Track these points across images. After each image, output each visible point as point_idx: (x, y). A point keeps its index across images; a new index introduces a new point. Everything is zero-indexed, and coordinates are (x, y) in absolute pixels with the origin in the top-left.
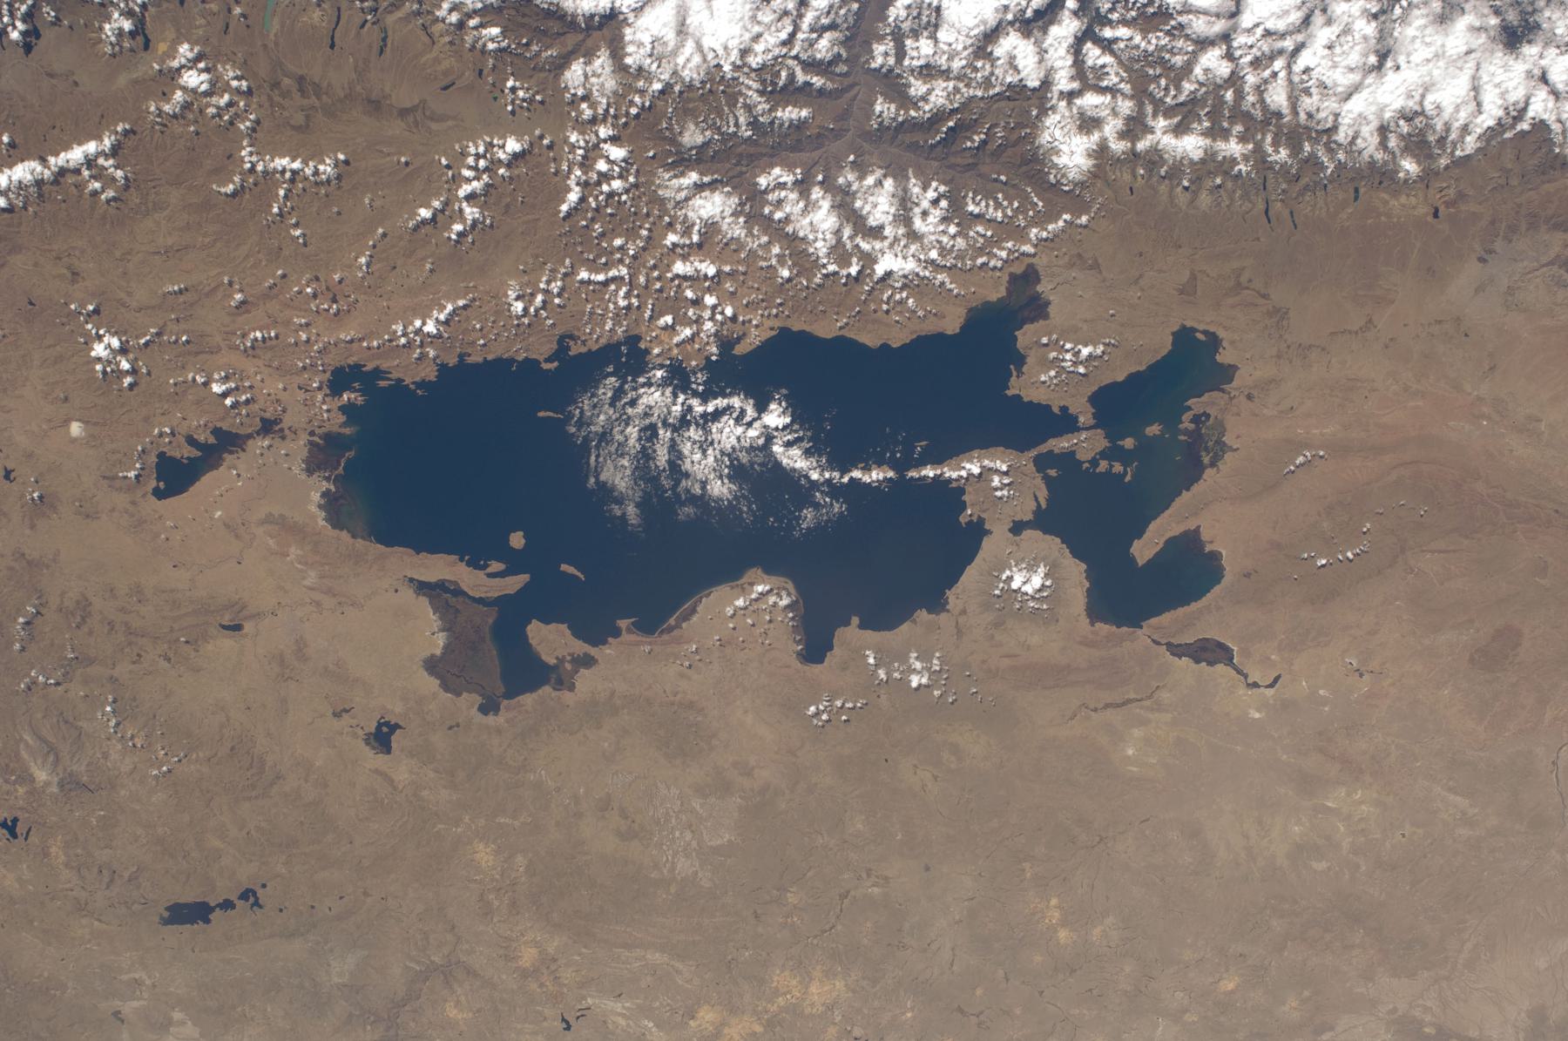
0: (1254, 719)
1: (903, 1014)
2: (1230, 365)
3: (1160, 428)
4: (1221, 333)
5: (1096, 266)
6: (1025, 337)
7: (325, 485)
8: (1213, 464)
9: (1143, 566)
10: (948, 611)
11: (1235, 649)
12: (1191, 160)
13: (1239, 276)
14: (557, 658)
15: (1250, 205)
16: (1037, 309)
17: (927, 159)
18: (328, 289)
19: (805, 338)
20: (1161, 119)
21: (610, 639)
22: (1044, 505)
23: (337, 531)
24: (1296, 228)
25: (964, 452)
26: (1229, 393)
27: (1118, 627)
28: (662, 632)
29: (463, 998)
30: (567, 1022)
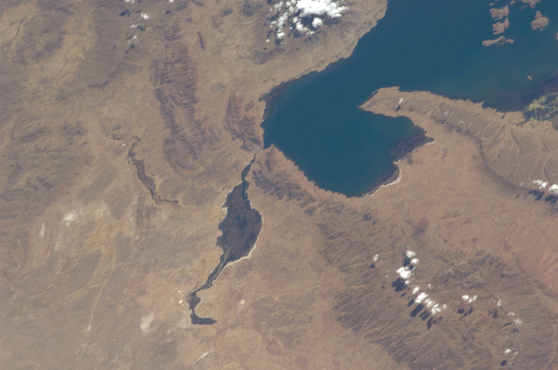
11: (250, 255)
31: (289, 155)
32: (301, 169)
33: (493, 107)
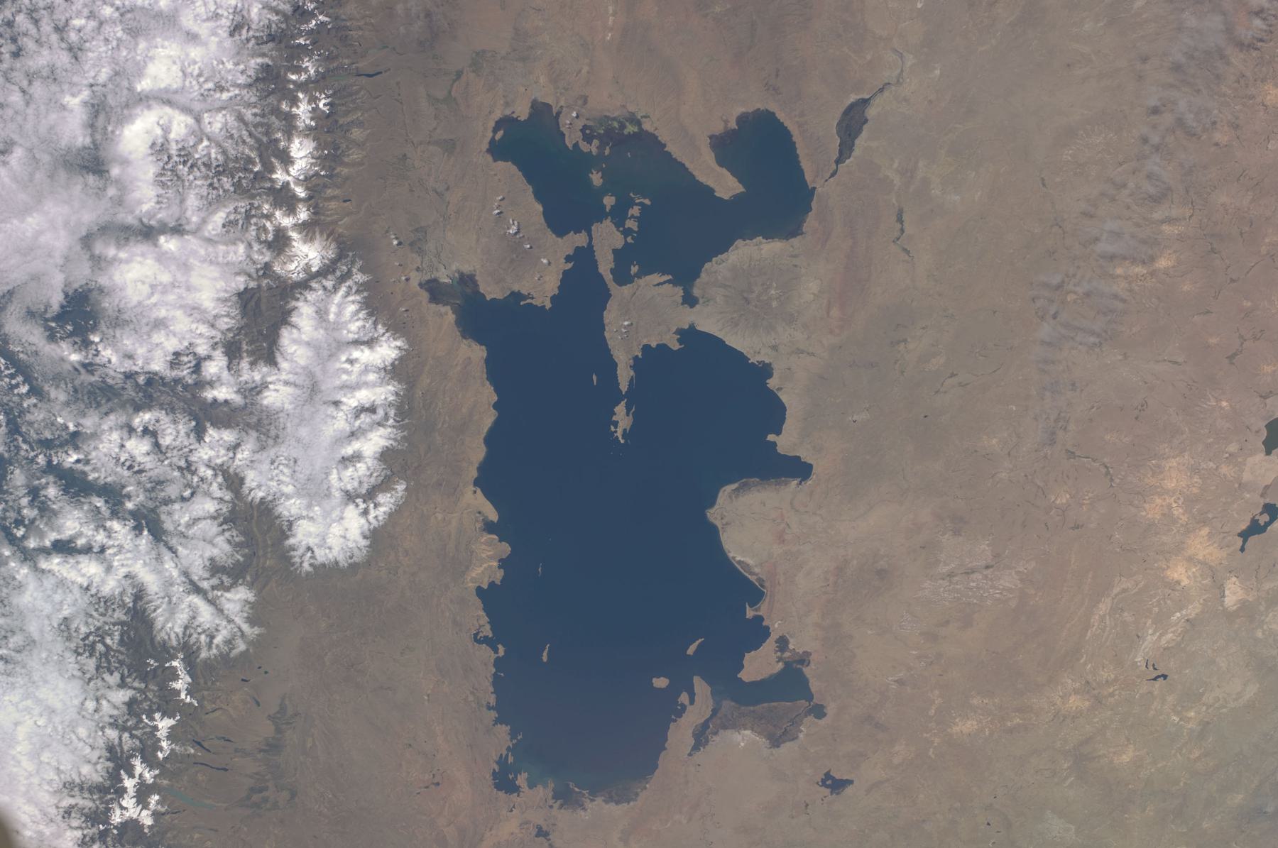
1: (1222, 408)
2: (532, 107)
3: (594, 172)
4: (497, 115)
6: (492, 291)
8: (639, 123)
9: (744, 186)
12: (316, 149)
14: (778, 662)
15: (362, 93)
16: (466, 280)
18: (427, 787)
20: (274, 176)
21: (764, 624)
22: (670, 277)
25: (607, 344)
26: (562, 107)
28: (762, 586)
29: (1112, 750)
30: (1159, 677)
33: (660, 142)
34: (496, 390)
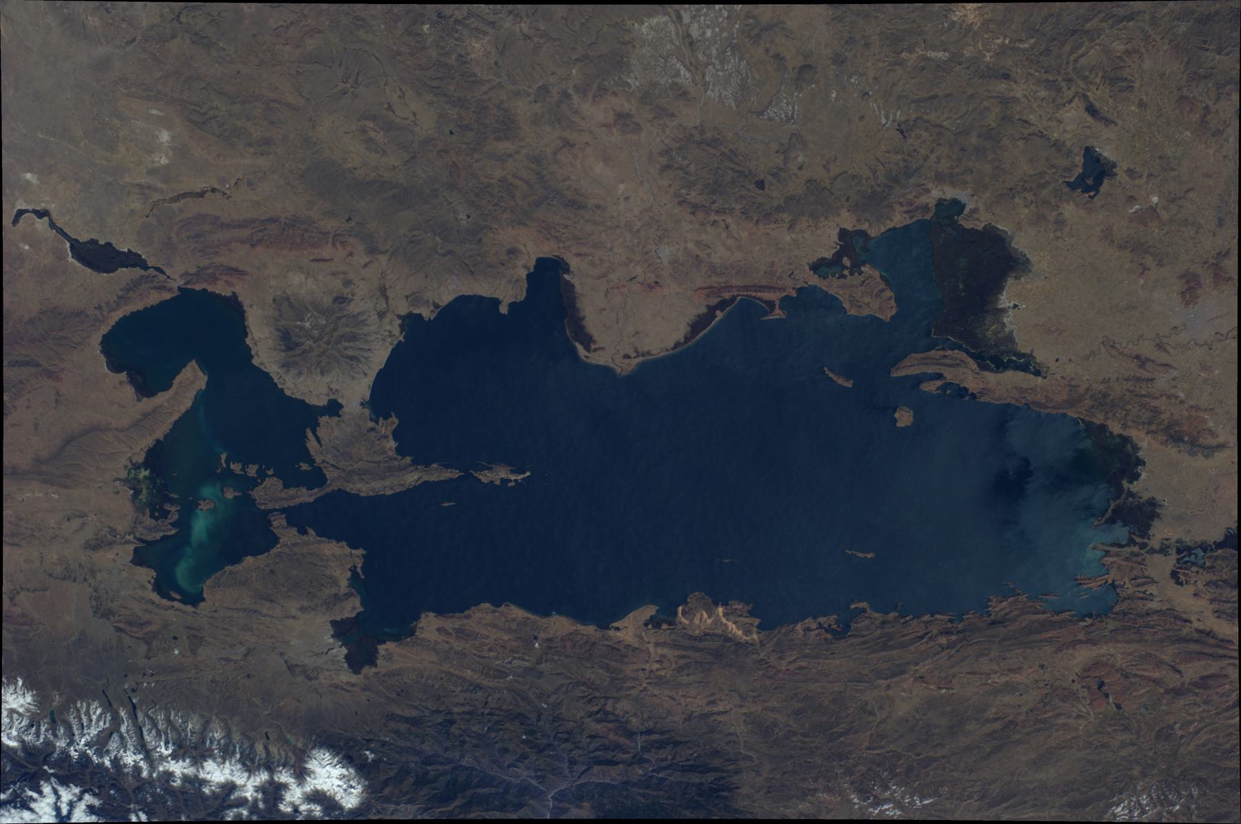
0: (30, 171)
2: (141, 565)
4: (155, 597)
5: (291, 668)
6: (352, 607)
7: (1135, 487)
8: (137, 467)
9: (191, 361)
10: (399, 317)
11: (70, 259)
12: (214, 760)
13: (149, 650)
14: (861, 273)
17: (473, 769)
18: (1107, 696)
19: (580, 615)
20: (250, 798)
23: (1125, 433)
24: (103, 691)
26: (135, 538)
27: (205, 290)
28: (733, 299)
31: (163, 304)
32: (146, 309)
33: (155, 446)
34: (477, 604)
